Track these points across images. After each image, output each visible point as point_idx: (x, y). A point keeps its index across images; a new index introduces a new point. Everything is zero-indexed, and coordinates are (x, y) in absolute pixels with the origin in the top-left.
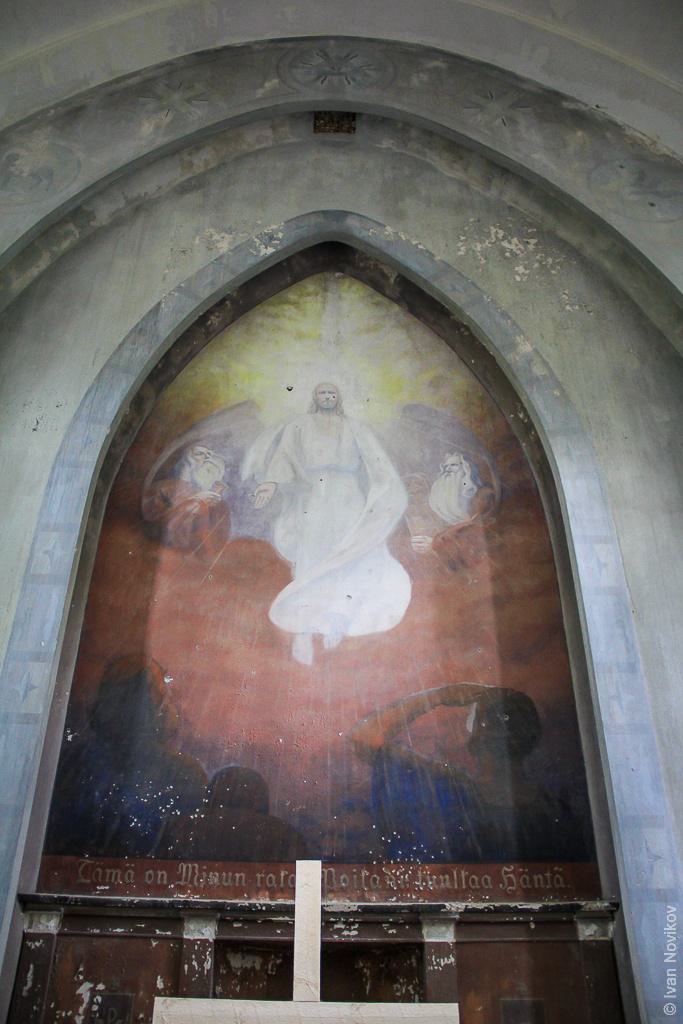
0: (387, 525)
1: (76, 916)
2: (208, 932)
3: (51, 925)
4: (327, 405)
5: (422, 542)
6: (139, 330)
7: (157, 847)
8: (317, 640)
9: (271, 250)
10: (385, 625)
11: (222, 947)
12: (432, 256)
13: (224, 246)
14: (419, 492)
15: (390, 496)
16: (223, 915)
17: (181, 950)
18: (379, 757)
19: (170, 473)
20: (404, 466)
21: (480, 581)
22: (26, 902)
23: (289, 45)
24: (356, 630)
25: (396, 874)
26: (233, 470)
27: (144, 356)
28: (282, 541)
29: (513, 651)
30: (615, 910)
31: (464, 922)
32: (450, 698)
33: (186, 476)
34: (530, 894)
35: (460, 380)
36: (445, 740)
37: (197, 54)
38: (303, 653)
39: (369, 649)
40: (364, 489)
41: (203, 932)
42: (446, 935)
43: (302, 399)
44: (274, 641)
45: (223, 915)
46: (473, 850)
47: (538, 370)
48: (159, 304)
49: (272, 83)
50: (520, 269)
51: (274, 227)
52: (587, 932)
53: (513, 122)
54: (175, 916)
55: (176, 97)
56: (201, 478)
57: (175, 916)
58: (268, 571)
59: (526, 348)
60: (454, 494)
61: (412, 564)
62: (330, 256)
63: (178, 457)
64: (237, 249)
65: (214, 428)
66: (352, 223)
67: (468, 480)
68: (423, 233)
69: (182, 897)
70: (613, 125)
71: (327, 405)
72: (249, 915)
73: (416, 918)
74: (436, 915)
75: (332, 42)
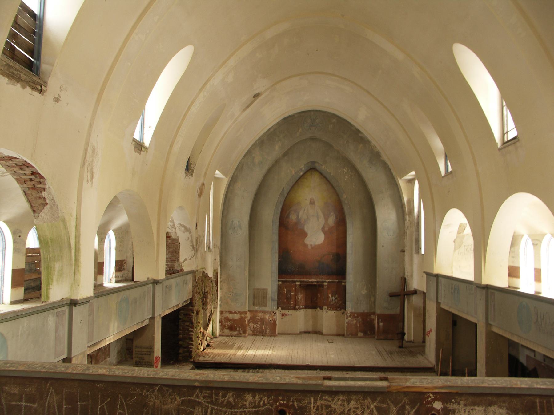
0: (321, 226)
1: (283, 282)
2: (299, 283)
3: (280, 283)
5: (326, 229)
6: (281, 194)
8: (311, 245)
9: (302, 173)
10: (320, 243)
11: (300, 285)
12: (330, 173)
13: (293, 172)
14: (326, 220)
15: (322, 221)
16: (301, 282)
17: (296, 285)
19: (288, 217)
20: (324, 215)
22: (278, 281)
23: (303, 114)
24: (317, 243)
25: (321, 276)
26: (298, 216)
27: (283, 199)
28: (306, 229)
30: (345, 282)
31: (329, 282)
33: (291, 217)
34: (337, 279)
37: (285, 119)
38: (309, 247)
39: (319, 246)
40: (318, 220)
41: (299, 283)
42: (327, 284)
43: (308, 202)
44: (305, 246)
45: (301, 282)
46: (330, 274)
47: (346, 202)
48: (283, 189)
49: (300, 130)
50: (346, 177)
51: (302, 167)
52: (343, 284)
54: (295, 282)
56: (293, 217)
57: (295, 282)
58: (304, 235)
59: (345, 197)
60: (332, 221)
62: (312, 169)
63: (289, 214)
64: (295, 173)
66: (316, 165)
67: (334, 218)
68: (329, 168)
69: (295, 280)
70: (369, 142)
71: (312, 203)
72: (304, 281)
73: (323, 282)
74: (325, 282)
75: (312, 113)
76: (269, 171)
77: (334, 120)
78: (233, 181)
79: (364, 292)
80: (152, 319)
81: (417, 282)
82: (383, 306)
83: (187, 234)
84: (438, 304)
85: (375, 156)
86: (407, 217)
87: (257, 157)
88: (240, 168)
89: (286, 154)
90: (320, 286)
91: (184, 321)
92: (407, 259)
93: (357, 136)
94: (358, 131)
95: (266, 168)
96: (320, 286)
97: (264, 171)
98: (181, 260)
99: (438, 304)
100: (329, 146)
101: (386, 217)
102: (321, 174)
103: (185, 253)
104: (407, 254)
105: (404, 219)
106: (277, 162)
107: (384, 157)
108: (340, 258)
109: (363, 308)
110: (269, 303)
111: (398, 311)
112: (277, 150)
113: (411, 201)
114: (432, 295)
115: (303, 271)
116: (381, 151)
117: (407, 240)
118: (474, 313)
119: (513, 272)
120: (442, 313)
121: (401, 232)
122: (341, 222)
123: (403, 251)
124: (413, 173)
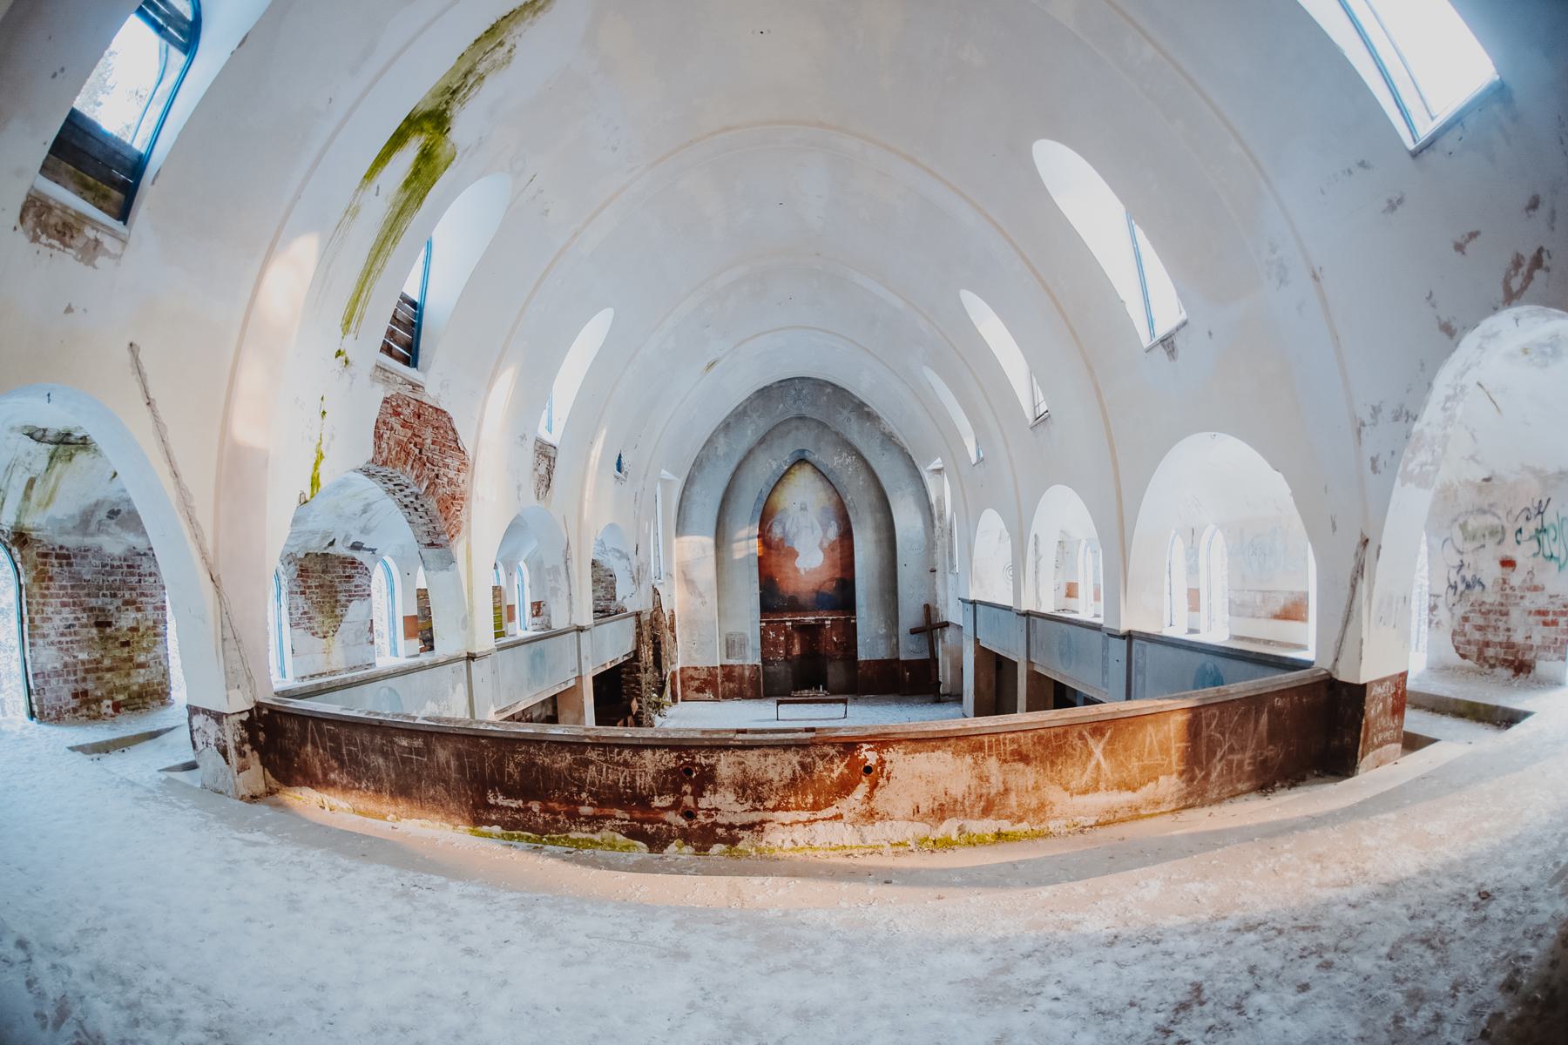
4: (803, 509)
5: (826, 545)
7: (780, 611)
14: (825, 531)
15: (819, 532)
18: (817, 592)
19: (770, 530)
21: (837, 554)
29: (843, 570)
32: (831, 580)
35: (835, 498)
36: (829, 588)
39: (816, 571)
43: (798, 506)
44: (796, 570)
46: (833, 608)
53: (849, 420)
55: (755, 416)
56: (777, 532)
58: (793, 554)
60: (833, 533)
61: (824, 551)
62: (801, 461)
65: (778, 517)
71: (803, 509)
76: (739, 467)
77: (829, 390)
78: (689, 482)
79: (882, 631)
80: (579, 678)
81: (952, 612)
82: (909, 650)
83: (624, 561)
84: (977, 641)
85: (889, 439)
86: (936, 522)
87: (722, 445)
88: (698, 464)
89: (762, 441)
90: (820, 625)
91: (629, 682)
92: (939, 581)
93: (862, 411)
94: (862, 405)
95: (735, 462)
96: (820, 625)
97: (733, 467)
98: (619, 598)
99: (977, 641)
100: (822, 425)
101: (907, 520)
102: (814, 467)
103: (623, 589)
104: (939, 574)
105: (933, 526)
106: (750, 452)
107: (901, 439)
108: (846, 583)
109: (881, 653)
110: (749, 653)
111: (926, 655)
112: (749, 434)
113: (940, 500)
114: (968, 630)
115: (794, 605)
116: (896, 431)
117: (938, 556)
118: (1011, 646)
119: (1071, 591)
120: (983, 654)
121: (930, 546)
122: (846, 535)
123: (933, 571)
124: (939, 460)
